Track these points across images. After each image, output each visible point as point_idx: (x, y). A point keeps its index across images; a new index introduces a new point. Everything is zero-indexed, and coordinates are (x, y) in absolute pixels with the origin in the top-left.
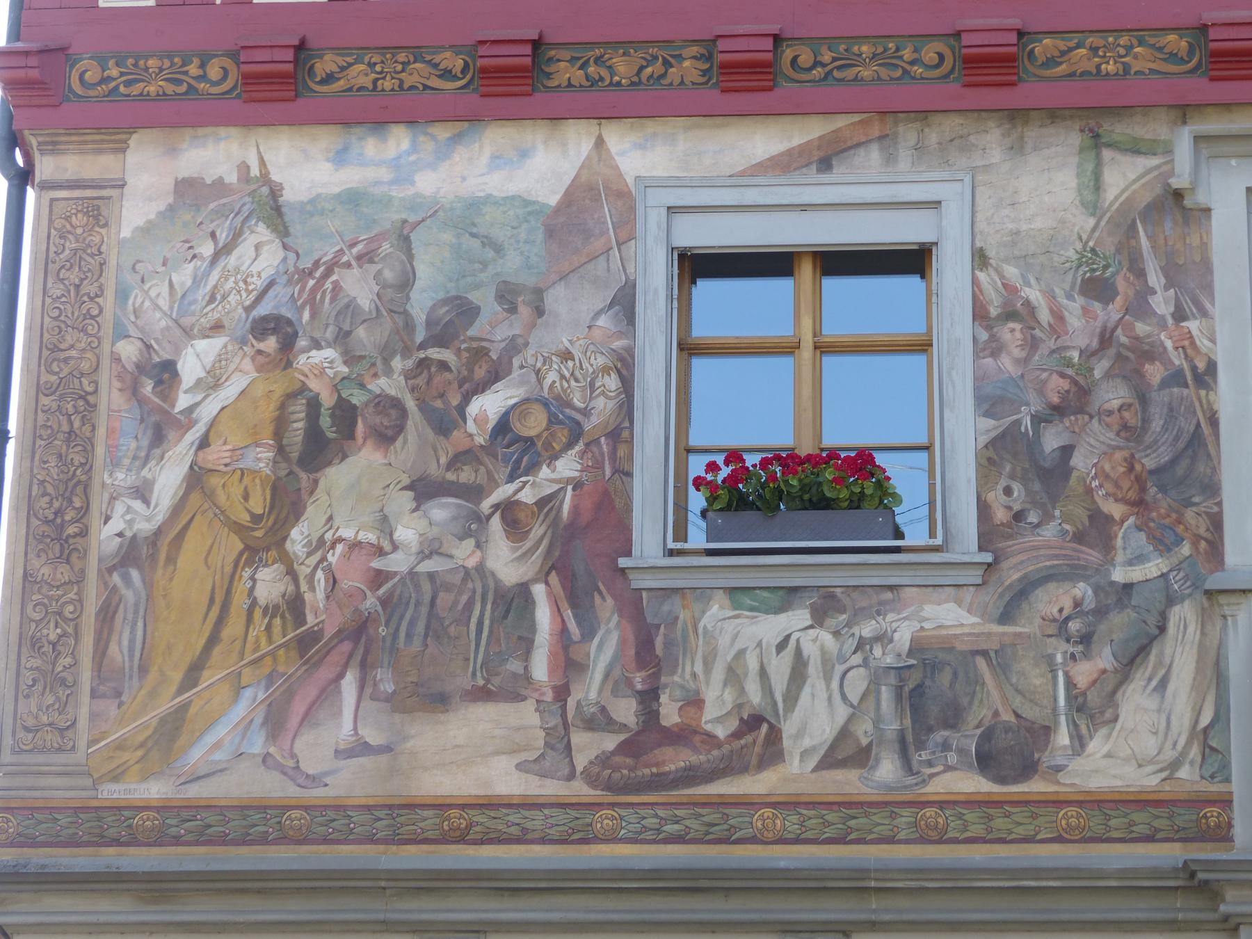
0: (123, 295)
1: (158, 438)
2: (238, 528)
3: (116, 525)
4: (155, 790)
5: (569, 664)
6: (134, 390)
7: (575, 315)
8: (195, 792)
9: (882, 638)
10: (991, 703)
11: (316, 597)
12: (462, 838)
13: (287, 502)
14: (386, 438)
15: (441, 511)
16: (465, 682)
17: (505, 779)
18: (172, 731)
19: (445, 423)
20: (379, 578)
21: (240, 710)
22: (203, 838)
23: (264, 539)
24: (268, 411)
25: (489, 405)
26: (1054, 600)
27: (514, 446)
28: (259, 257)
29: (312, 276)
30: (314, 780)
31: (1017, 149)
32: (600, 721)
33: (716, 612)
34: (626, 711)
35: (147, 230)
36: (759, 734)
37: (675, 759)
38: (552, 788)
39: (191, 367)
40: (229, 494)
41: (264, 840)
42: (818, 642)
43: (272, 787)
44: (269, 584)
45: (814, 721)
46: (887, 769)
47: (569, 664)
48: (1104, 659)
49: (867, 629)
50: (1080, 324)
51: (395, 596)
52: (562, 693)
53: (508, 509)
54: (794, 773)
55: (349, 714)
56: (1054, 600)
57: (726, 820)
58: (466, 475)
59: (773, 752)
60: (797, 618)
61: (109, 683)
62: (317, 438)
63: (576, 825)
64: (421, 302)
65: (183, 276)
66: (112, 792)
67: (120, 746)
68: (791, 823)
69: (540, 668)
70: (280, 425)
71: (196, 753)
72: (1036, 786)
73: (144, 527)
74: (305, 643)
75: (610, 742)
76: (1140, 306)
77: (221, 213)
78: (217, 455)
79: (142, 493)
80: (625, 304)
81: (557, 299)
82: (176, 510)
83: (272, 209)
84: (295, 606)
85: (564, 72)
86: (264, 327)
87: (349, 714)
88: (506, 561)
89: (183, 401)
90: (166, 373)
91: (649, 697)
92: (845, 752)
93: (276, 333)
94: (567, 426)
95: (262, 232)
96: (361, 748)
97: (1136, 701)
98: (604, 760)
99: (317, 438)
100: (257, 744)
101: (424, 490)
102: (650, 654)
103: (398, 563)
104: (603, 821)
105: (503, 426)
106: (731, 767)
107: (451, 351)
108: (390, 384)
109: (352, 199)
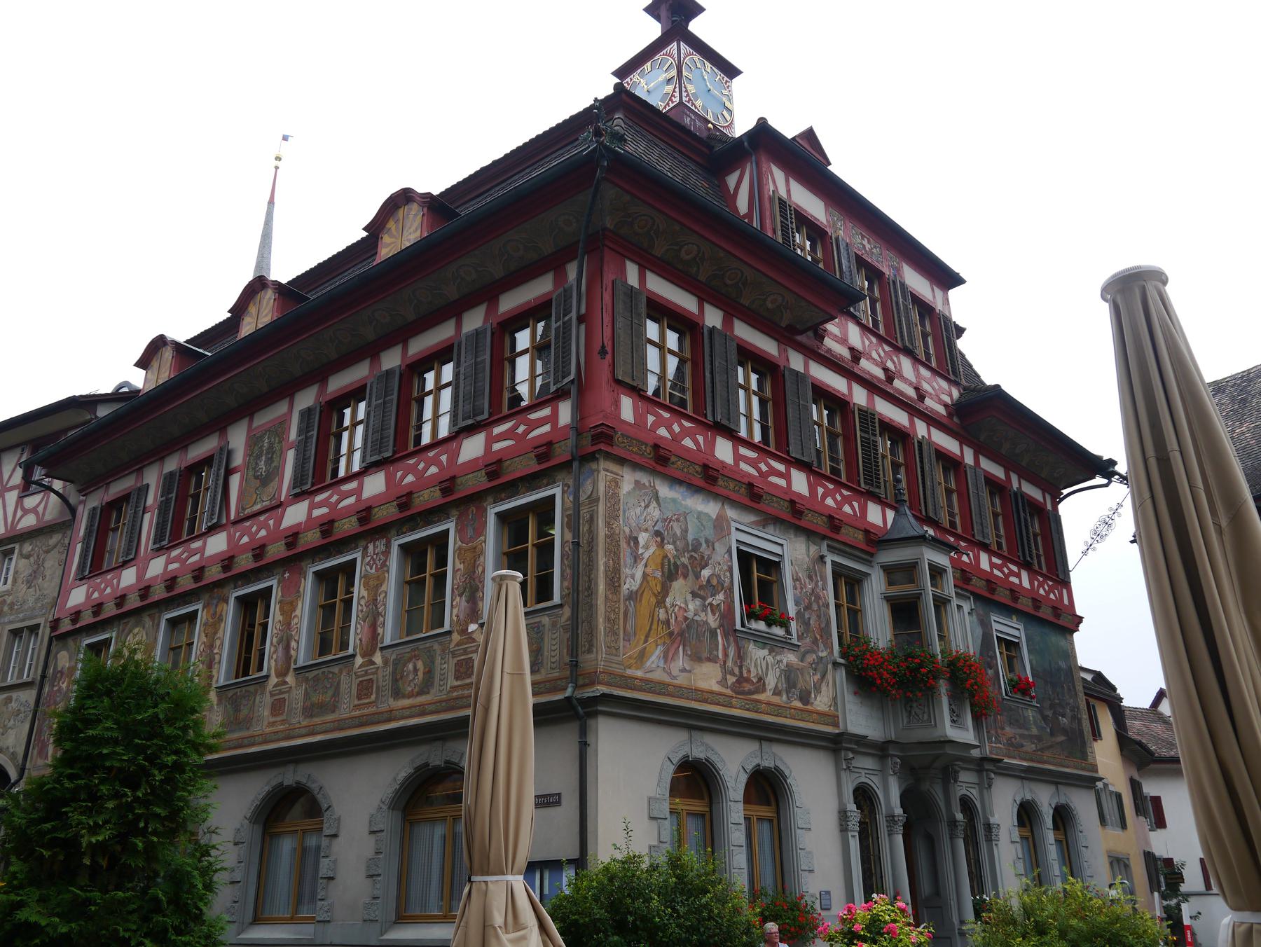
0: (624, 511)
1: (635, 561)
2: (656, 596)
3: (627, 586)
4: (639, 674)
5: (726, 655)
6: (629, 544)
8: (649, 676)
9: (781, 661)
11: (672, 621)
12: (705, 701)
13: (665, 591)
14: (685, 576)
15: (698, 602)
16: (705, 655)
17: (716, 688)
18: (642, 656)
19: (698, 576)
20: (686, 618)
21: (657, 652)
22: (650, 691)
23: (661, 603)
24: (659, 561)
25: (706, 573)
26: (811, 658)
30: (675, 678)
31: (796, 536)
32: (732, 673)
33: (751, 646)
34: (737, 671)
35: (629, 493)
37: (747, 687)
38: (724, 690)
39: (642, 541)
40: (652, 583)
41: (664, 694)
42: (770, 659)
43: (667, 679)
44: (662, 614)
45: (771, 682)
46: (784, 697)
47: (726, 655)
48: (818, 677)
49: (778, 658)
51: (690, 624)
52: (725, 662)
53: (711, 604)
55: (681, 661)
56: (811, 658)
57: (755, 706)
58: (702, 593)
59: (764, 690)
60: (766, 652)
61: (627, 638)
62: (671, 572)
64: (690, 537)
65: (638, 510)
66: (629, 672)
67: (630, 657)
68: (768, 709)
69: (720, 656)
70: (662, 565)
71: (648, 664)
72: (809, 707)
73: (634, 589)
74: (671, 634)
75: (734, 679)
76: (816, 584)
77: (645, 494)
78: (649, 570)
79: (633, 577)
80: (729, 551)
81: (717, 545)
82: (641, 584)
84: (667, 622)
85: (720, 482)
86: (658, 533)
87: (681, 661)
88: (713, 621)
89: (640, 551)
90: (636, 540)
91: (741, 667)
92: (777, 692)
95: (654, 504)
96: (683, 670)
97: (824, 688)
98: (733, 684)
99: (671, 572)
100: (662, 664)
101: (695, 595)
102: (741, 656)
103: (690, 615)
104: (734, 702)
105: (708, 581)
106: (756, 692)
108: (685, 560)
109: (674, 500)
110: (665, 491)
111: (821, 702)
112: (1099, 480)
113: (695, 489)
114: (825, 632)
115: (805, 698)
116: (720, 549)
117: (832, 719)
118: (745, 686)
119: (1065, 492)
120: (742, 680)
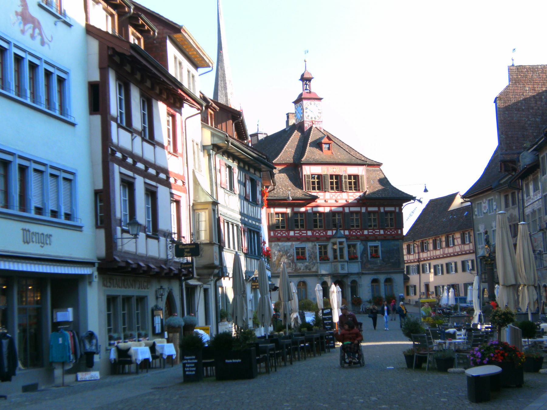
7: (292, 250)
10: (309, 267)
27: (290, 256)
28: (278, 247)
29: (280, 248)
36: (300, 269)
45: (302, 268)
50: (312, 250)
54: (301, 270)
57: (299, 273)
63: (293, 273)
83: (279, 245)
92: (303, 270)
93: (279, 251)
94: (292, 255)
102: (296, 266)
107: (286, 252)
110: (280, 243)
111: (314, 269)
112: (412, 201)
113: (286, 241)
114: (316, 257)
115: (310, 269)
116: (292, 250)
117: (317, 272)
118: (296, 270)
119: (404, 204)
120: (296, 269)
